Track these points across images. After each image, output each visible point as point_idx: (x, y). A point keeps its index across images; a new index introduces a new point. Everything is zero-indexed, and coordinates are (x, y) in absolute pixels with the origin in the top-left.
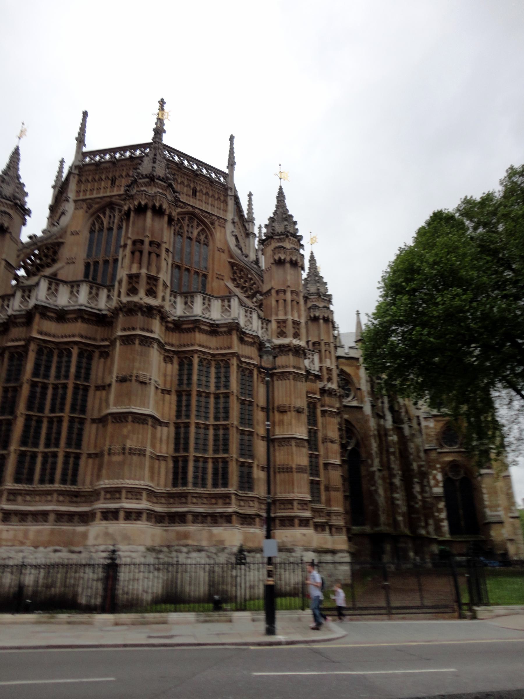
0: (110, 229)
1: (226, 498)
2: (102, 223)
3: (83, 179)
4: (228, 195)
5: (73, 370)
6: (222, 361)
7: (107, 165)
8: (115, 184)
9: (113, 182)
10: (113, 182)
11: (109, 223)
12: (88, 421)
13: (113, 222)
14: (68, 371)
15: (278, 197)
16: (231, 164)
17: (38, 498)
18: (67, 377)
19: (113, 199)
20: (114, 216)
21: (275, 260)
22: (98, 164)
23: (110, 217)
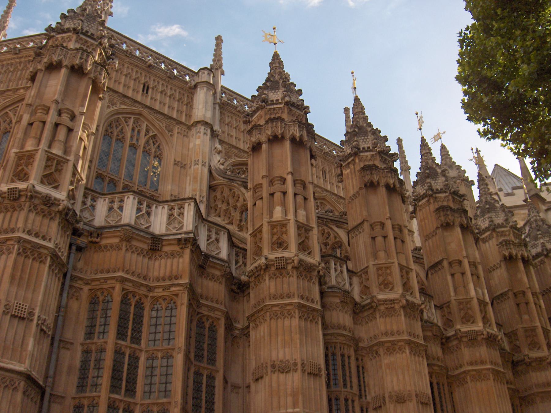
0: (133, 147)
2: (122, 131)
8: (147, 93)
9: (146, 89)
10: (146, 89)
11: (132, 137)
23: (133, 129)
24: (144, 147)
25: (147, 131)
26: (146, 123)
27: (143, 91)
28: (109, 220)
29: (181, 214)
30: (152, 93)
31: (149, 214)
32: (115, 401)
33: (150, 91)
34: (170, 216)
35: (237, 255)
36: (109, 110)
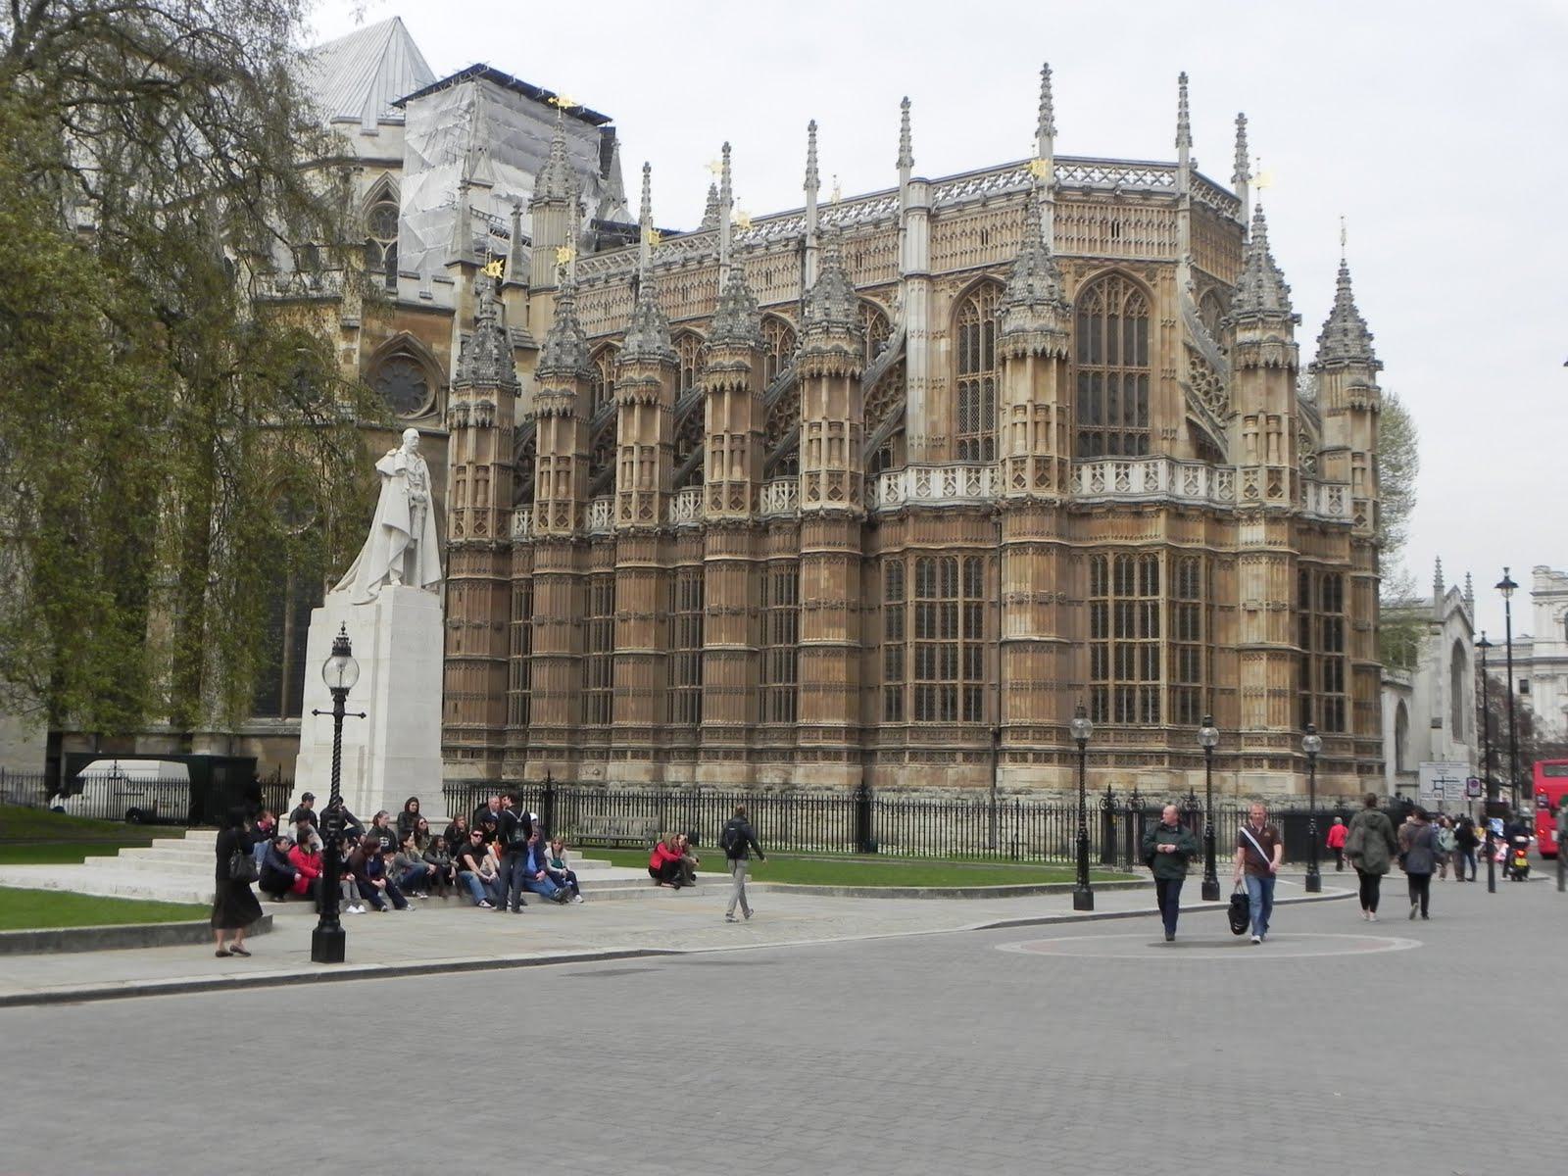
0: (1113, 318)
1: (1343, 744)
2: (1097, 302)
3: (1064, 214)
4: (1242, 244)
5: (1202, 586)
6: (1332, 573)
7: (1102, 196)
10: (1116, 229)
11: (1109, 305)
12: (1216, 651)
13: (1116, 305)
14: (1195, 588)
15: (1338, 282)
16: (1242, 177)
17: (1184, 739)
18: (1195, 595)
19: (1122, 266)
20: (1116, 293)
21: (1353, 407)
22: (1087, 191)
24: (1125, 312)
25: (1126, 288)
26: (1123, 279)
27: (1113, 235)
28: (1094, 488)
29: (1156, 473)
30: (1124, 235)
31: (1127, 475)
32: (1120, 643)
33: (1121, 231)
34: (1147, 475)
35: (1222, 475)
36: (1078, 287)
